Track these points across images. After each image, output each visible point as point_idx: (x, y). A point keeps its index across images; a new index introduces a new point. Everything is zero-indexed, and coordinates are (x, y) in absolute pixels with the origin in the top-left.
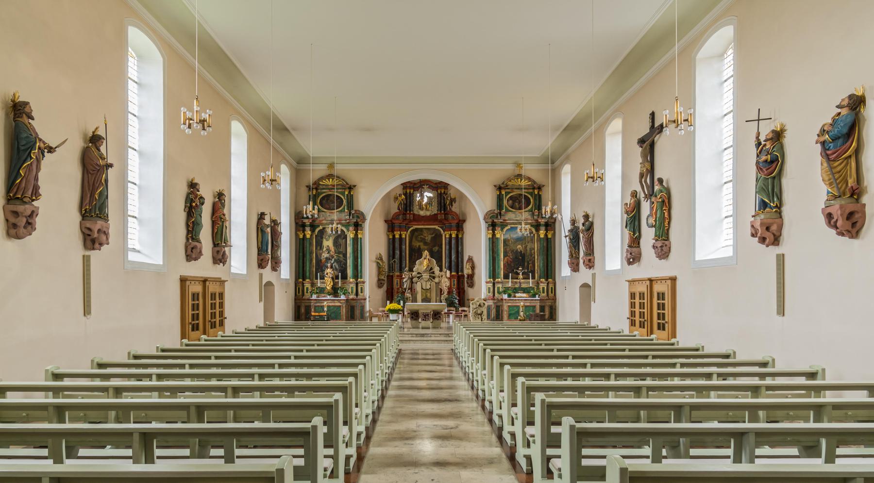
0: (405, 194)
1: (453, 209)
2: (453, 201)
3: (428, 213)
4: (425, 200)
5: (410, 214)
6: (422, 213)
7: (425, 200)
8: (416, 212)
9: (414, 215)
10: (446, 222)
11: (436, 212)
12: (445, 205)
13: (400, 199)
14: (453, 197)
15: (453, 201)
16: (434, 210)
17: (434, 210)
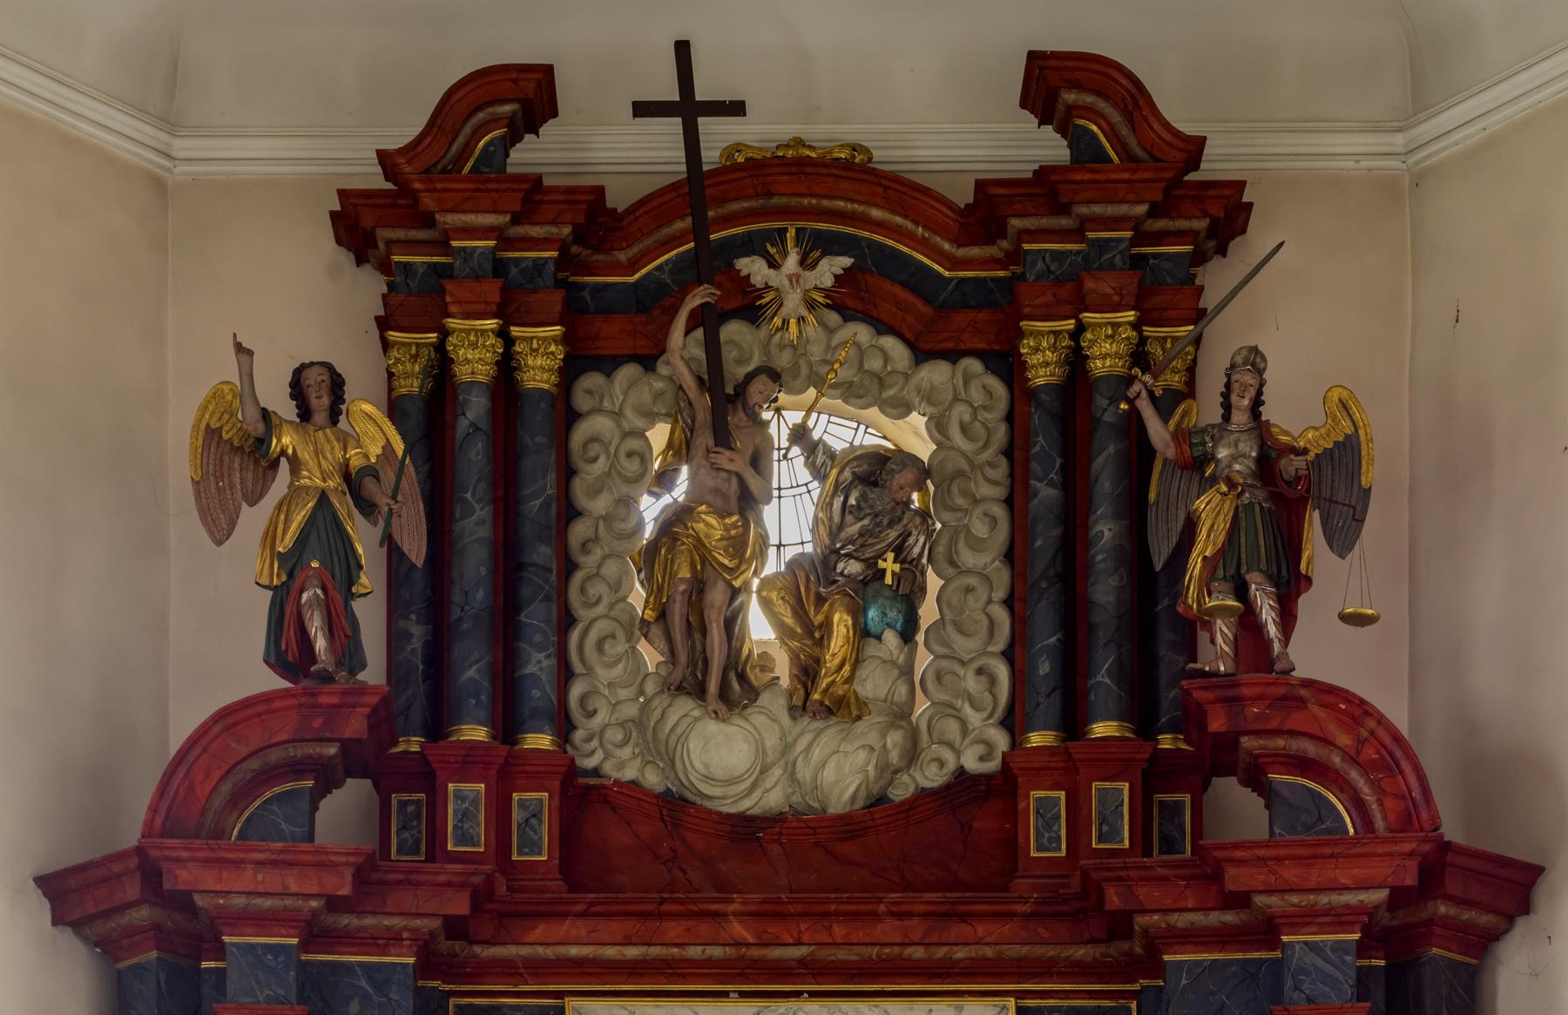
0: (429, 414)
1: (1317, 650)
2: (1299, 495)
3: (840, 769)
4: (792, 518)
5: (505, 770)
6: (727, 760)
7: (792, 518)
8: (615, 758)
9: (581, 795)
10: (1171, 910)
11: (976, 745)
12: (1151, 584)
13: (312, 459)
14: (1295, 414)
15: (1299, 495)
16: (942, 699)
17: (942, 699)
